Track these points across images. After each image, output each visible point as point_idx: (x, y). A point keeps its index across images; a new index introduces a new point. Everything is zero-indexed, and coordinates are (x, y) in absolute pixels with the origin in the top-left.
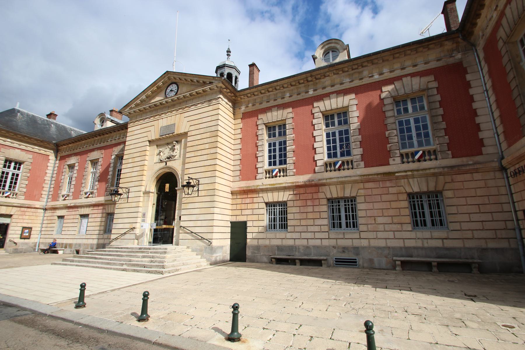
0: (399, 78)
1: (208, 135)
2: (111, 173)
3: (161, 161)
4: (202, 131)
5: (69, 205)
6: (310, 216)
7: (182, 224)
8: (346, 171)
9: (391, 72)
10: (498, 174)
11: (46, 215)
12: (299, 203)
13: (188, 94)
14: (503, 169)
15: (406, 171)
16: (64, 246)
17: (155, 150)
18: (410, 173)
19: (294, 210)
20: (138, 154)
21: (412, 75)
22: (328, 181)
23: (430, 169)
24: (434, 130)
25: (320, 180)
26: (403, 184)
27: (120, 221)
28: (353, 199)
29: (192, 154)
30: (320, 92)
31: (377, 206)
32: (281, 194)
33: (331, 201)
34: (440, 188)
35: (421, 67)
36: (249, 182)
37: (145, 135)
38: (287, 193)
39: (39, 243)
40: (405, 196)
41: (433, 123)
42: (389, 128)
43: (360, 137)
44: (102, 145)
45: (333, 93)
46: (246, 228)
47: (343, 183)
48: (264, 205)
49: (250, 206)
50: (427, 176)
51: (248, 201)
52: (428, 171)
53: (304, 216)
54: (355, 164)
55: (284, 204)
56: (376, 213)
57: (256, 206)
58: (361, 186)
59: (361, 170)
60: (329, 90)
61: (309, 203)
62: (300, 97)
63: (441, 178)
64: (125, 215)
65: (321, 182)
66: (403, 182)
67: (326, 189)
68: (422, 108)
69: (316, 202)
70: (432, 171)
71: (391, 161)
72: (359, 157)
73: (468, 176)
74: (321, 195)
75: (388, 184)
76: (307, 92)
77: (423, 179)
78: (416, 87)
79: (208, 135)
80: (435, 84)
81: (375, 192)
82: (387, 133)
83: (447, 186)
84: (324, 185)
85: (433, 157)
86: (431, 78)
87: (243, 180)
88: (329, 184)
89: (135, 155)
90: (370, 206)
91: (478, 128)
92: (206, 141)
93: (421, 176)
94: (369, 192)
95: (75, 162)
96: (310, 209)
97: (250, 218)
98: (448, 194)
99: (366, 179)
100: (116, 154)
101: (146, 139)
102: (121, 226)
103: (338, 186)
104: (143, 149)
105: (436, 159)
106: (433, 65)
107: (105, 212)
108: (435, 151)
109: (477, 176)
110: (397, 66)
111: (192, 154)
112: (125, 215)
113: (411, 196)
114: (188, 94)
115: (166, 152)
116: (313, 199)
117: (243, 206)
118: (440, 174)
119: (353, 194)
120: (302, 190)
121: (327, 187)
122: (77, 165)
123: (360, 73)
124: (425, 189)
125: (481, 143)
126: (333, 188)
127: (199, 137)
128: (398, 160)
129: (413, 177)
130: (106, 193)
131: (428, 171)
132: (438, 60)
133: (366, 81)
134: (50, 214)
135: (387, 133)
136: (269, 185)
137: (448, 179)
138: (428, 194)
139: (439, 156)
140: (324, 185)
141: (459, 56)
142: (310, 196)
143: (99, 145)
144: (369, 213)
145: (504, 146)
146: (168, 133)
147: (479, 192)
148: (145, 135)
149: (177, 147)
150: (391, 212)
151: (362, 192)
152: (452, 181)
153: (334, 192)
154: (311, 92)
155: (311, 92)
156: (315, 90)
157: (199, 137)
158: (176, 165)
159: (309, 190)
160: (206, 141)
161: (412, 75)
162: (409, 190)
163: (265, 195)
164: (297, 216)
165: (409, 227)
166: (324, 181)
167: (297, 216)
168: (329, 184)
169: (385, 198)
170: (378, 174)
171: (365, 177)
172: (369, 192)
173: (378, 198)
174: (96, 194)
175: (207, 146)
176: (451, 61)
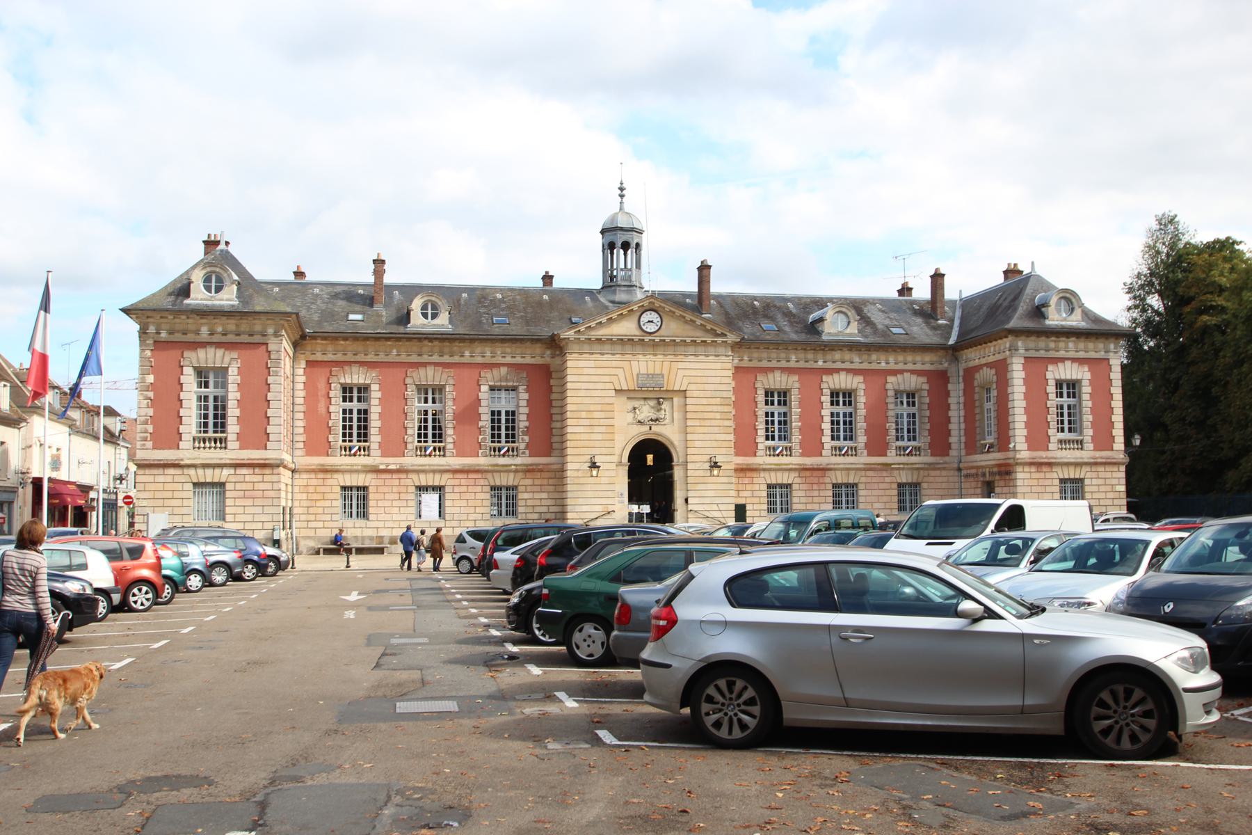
0: (901, 372)
1: (718, 401)
2: (483, 417)
3: (639, 421)
4: (708, 394)
5: (382, 467)
6: (816, 500)
7: (690, 507)
8: (850, 457)
9: (895, 363)
10: (956, 473)
11: (296, 482)
12: (804, 487)
13: (688, 340)
14: (959, 470)
15: (899, 464)
16: (386, 541)
17: (623, 404)
18: (902, 466)
19: (801, 493)
20: (599, 408)
21: (913, 372)
22: (836, 466)
23: (916, 464)
24: (920, 427)
25: (828, 464)
26: (895, 474)
27: (580, 501)
28: (854, 485)
29: (697, 423)
30: (830, 365)
31: (875, 493)
32: (786, 474)
33: (835, 486)
34: (920, 481)
35: (919, 367)
36: (748, 458)
37: (607, 379)
38: (793, 474)
39: (296, 537)
40: (895, 486)
41: (921, 423)
42: (890, 420)
43: (865, 424)
44: (446, 359)
45: (843, 370)
46: (745, 511)
47: (848, 469)
48: (766, 486)
49: (749, 487)
50: (912, 469)
51: (746, 481)
52: (914, 466)
53: (810, 500)
54: (859, 452)
55: (788, 486)
56: (873, 499)
57: (757, 487)
58: (863, 473)
59: (864, 459)
60: (839, 365)
61: (815, 487)
62: (807, 365)
63: (922, 471)
64: (590, 494)
65: (829, 467)
66: (896, 473)
67: (831, 474)
68: (914, 404)
69: (822, 487)
70: (917, 466)
71: (889, 454)
72: (863, 445)
73: (938, 473)
74: (827, 480)
75: (884, 474)
76: (816, 362)
77: (910, 472)
78: (913, 385)
79: (718, 401)
80: (926, 387)
81: (874, 480)
82: (888, 425)
83: (925, 479)
84: (830, 469)
85: (918, 453)
86: (924, 379)
87: (737, 454)
88: (835, 470)
89: (592, 408)
90: (869, 493)
91: (948, 433)
92: (715, 408)
93: (909, 469)
94: (869, 480)
95: (368, 382)
96: (816, 493)
97: (749, 500)
98: (924, 485)
99: (869, 468)
100: (490, 383)
101: (610, 386)
102: (585, 508)
103: (843, 472)
104: (607, 400)
105: (920, 455)
106: (928, 367)
107: (487, 484)
108: (919, 448)
109: (944, 473)
110: (901, 358)
111: (697, 423)
112: (590, 494)
113: (900, 485)
114: (688, 340)
115: (646, 412)
116: (819, 483)
117: (741, 487)
118: (922, 469)
119: (856, 481)
120: (808, 473)
121: (833, 472)
122: (375, 387)
123: (869, 355)
124: (910, 481)
125: (949, 446)
126: (838, 473)
127: (705, 401)
128: (894, 452)
129: (903, 469)
130: (480, 451)
131: (914, 466)
132: (932, 364)
133: (874, 366)
134: (314, 482)
135: (888, 425)
136: (775, 464)
137: (926, 473)
138: (910, 485)
139: (922, 454)
140: (830, 469)
141: (946, 365)
142: (815, 480)
143: (436, 358)
144: (869, 499)
145: (963, 453)
146: (653, 385)
147: (944, 486)
148: (607, 379)
149: (666, 405)
150: (885, 499)
151: (863, 479)
152: (929, 476)
153: (840, 478)
154: (820, 363)
155: (820, 363)
156: (825, 362)
157: (705, 401)
158: (669, 432)
159: (816, 473)
160: (715, 408)
161: (913, 372)
162: (899, 481)
163: (766, 474)
164: (803, 500)
165: (896, 512)
166: (832, 466)
167: (803, 500)
168: (835, 470)
169: (882, 486)
170: (879, 464)
171: (868, 466)
172: (869, 480)
173: (876, 486)
174: (454, 451)
175: (718, 416)
176: (940, 367)
